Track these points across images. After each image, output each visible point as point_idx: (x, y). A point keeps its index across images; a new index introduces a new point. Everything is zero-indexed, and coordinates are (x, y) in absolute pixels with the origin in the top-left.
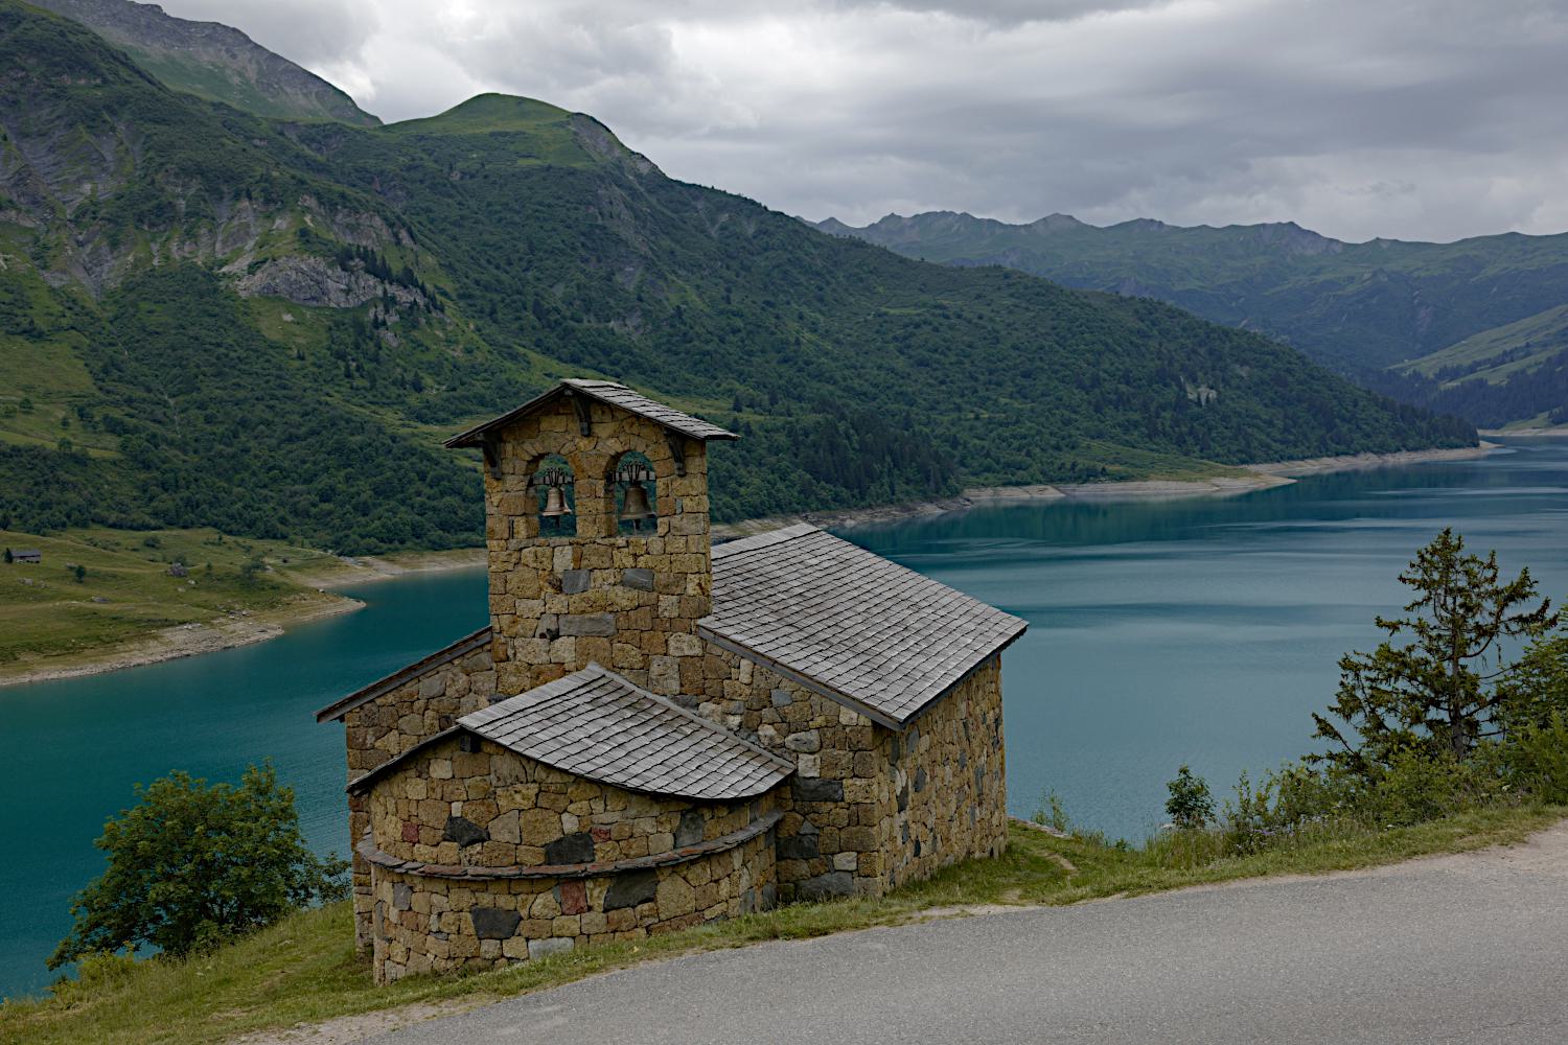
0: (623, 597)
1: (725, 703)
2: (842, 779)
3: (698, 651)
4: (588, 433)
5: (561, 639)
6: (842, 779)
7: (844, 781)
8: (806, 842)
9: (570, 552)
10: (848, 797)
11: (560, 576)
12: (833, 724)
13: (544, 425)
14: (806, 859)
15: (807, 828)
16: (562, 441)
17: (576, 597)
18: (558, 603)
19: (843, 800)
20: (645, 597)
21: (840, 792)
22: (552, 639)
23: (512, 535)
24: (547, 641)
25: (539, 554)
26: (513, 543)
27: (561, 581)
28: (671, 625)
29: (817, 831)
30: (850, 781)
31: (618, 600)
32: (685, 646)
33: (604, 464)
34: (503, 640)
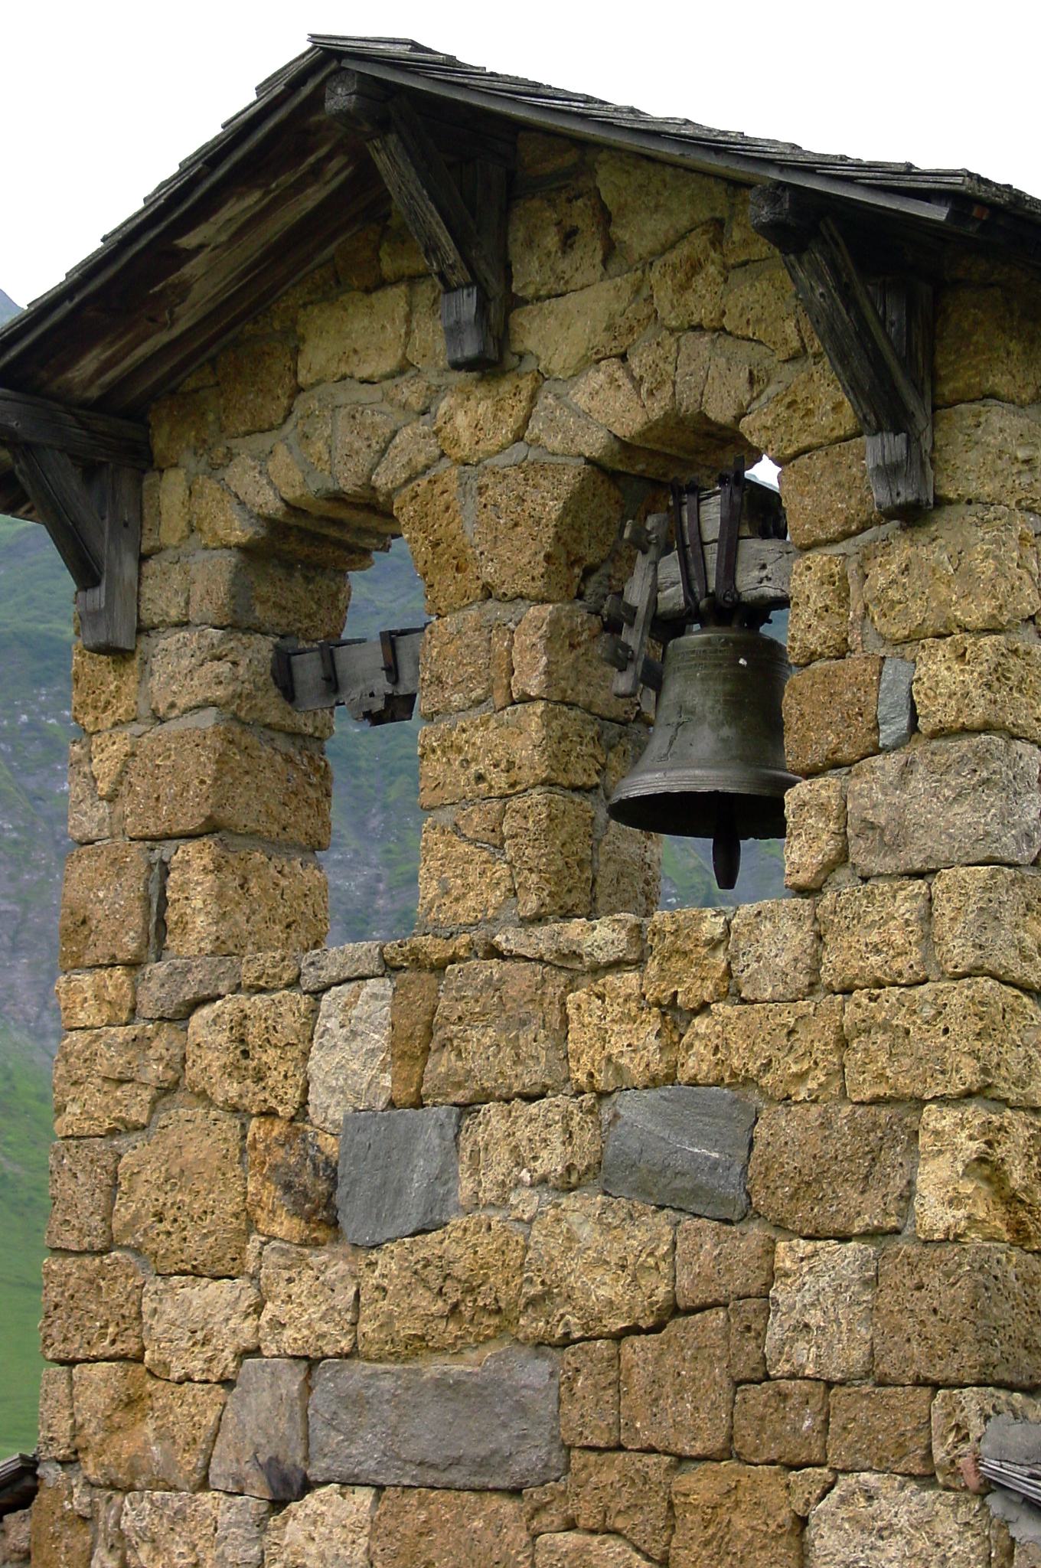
0: (602, 1255)
4: (491, 361)
5: (311, 1502)
9: (383, 1011)
11: (330, 1145)
13: (317, 357)
16: (381, 420)
17: (388, 1263)
18: (310, 1301)
20: (708, 1254)
22: (277, 1505)
23: (158, 931)
24: (253, 1503)
25: (254, 1030)
26: (157, 986)
27: (331, 1172)
31: (575, 1273)
33: (554, 509)
34: (79, 1501)
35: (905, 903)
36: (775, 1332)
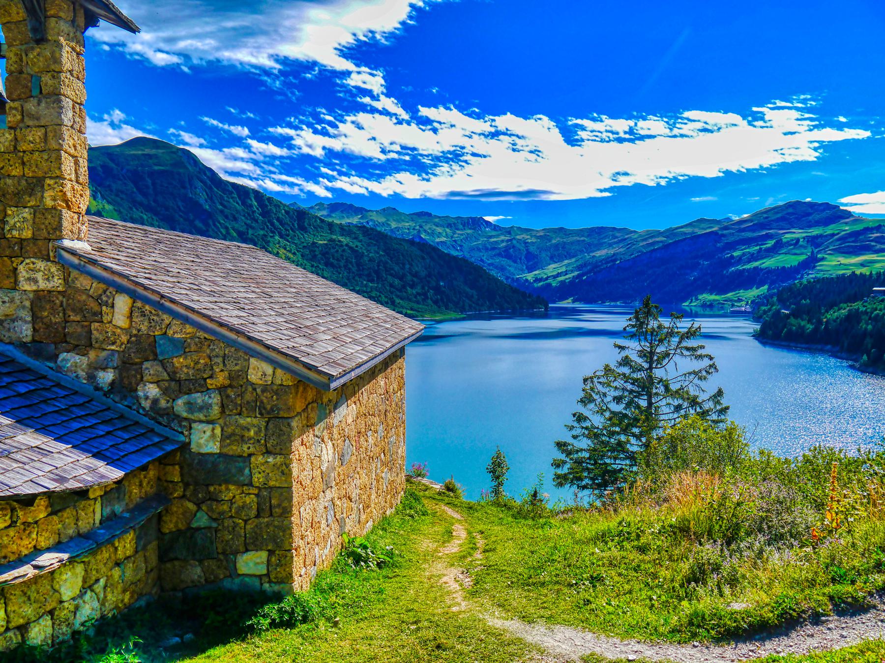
1: (92, 354)
2: (250, 455)
3: (57, 283)
6: (250, 455)
7: (253, 459)
8: (199, 537)
10: (258, 479)
12: (238, 379)
14: (201, 562)
15: (202, 520)
19: (251, 484)
21: (247, 471)
28: (22, 249)
29: (214, 525)
30: (260, 459)
32: (39, 276)
35: (40, 133)
36: (7, 228)
